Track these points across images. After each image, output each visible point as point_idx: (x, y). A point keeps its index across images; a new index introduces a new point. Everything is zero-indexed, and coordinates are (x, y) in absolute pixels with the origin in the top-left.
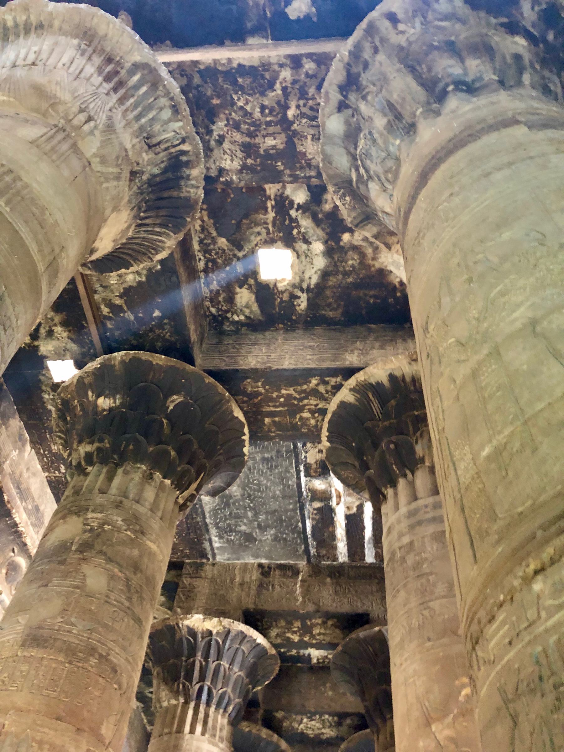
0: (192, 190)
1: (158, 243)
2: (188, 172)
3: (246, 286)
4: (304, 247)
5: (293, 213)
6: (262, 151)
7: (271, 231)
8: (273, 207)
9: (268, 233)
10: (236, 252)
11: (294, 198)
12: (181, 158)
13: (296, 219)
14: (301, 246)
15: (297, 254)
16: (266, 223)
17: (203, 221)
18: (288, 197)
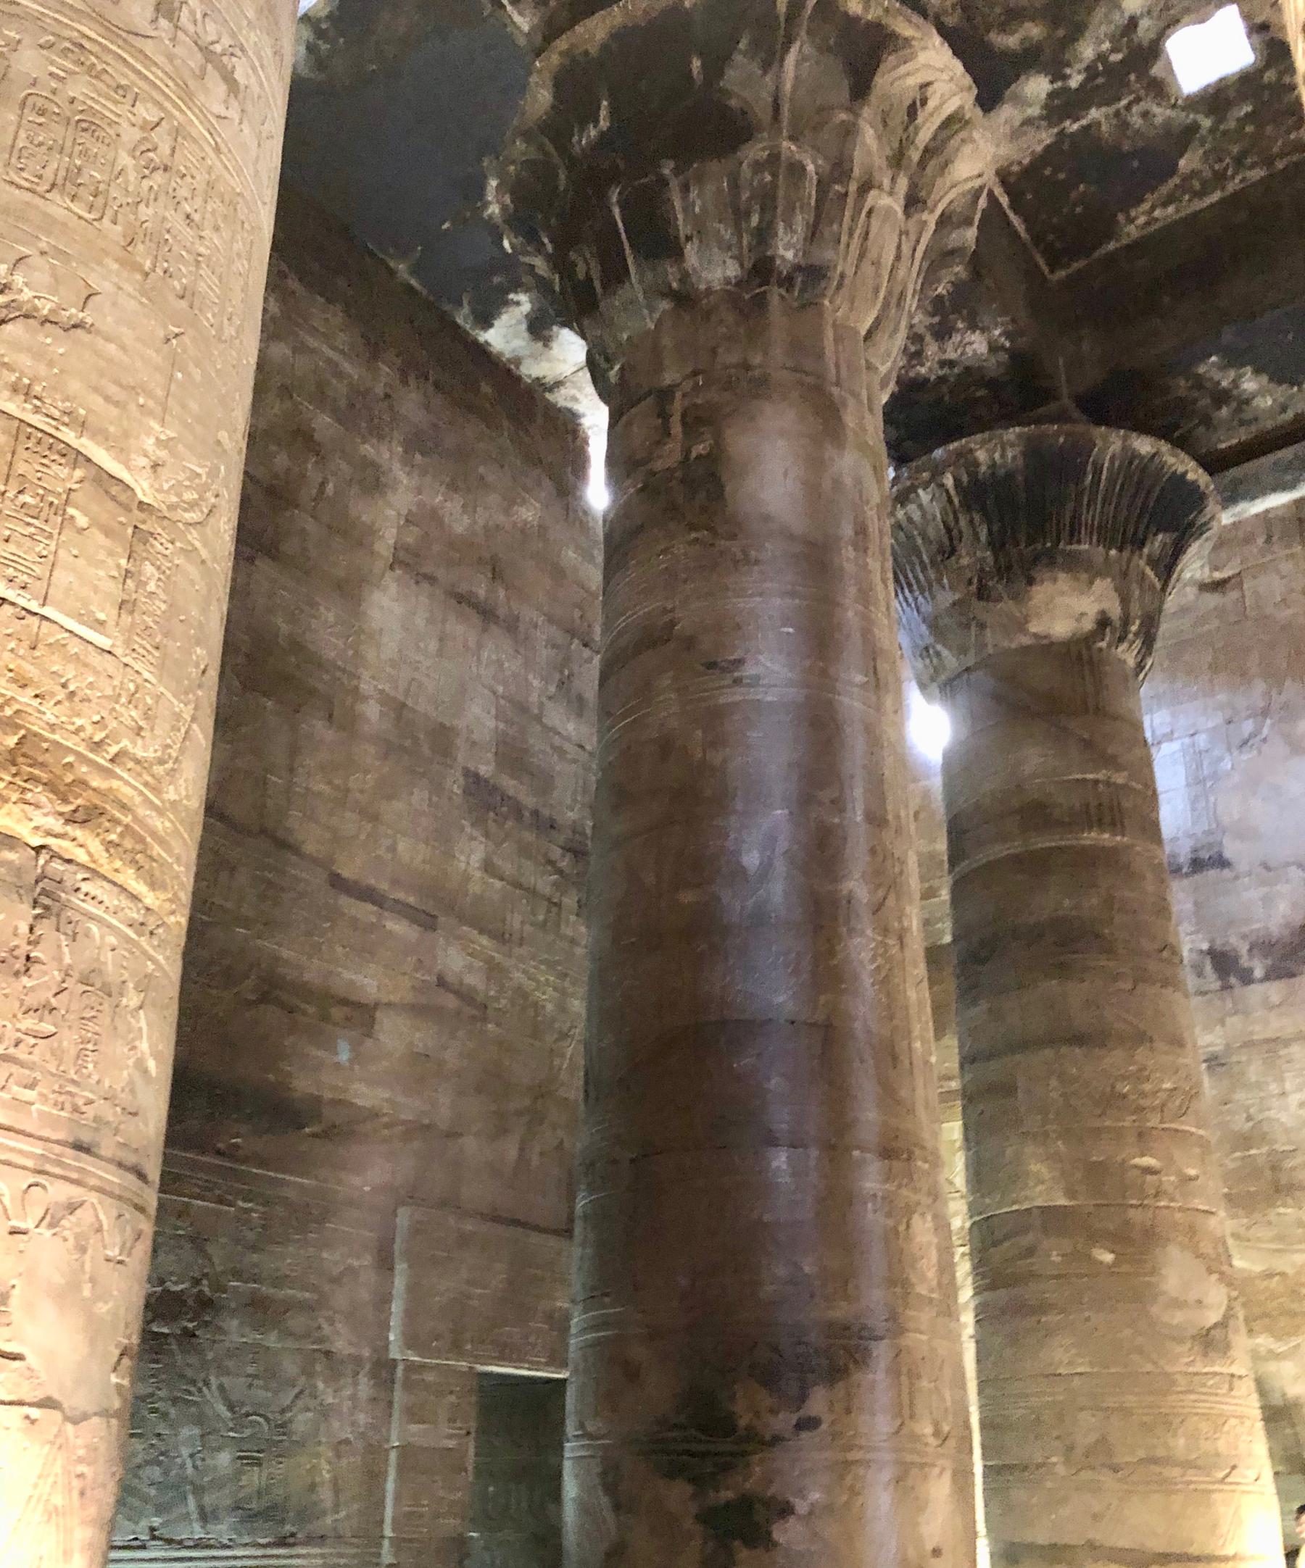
0: (1010, 455)
1: (1117, 464)
2: (983, 469)
3: (1287, 80)
4: (1144, 24)
5: (1075, 81)
6: (937, 319)
7: (1131, 97)
8: (1077, 119)
9: (1138, 100)
10: (1203, 132)
11: (1043, 96)
12: (965, 484)
13: (1088, 69)
14: (1146, 28)
15: (1168, 26)
16: (1117, 114)
17: (1153, 208)
18: (1046, 107)
